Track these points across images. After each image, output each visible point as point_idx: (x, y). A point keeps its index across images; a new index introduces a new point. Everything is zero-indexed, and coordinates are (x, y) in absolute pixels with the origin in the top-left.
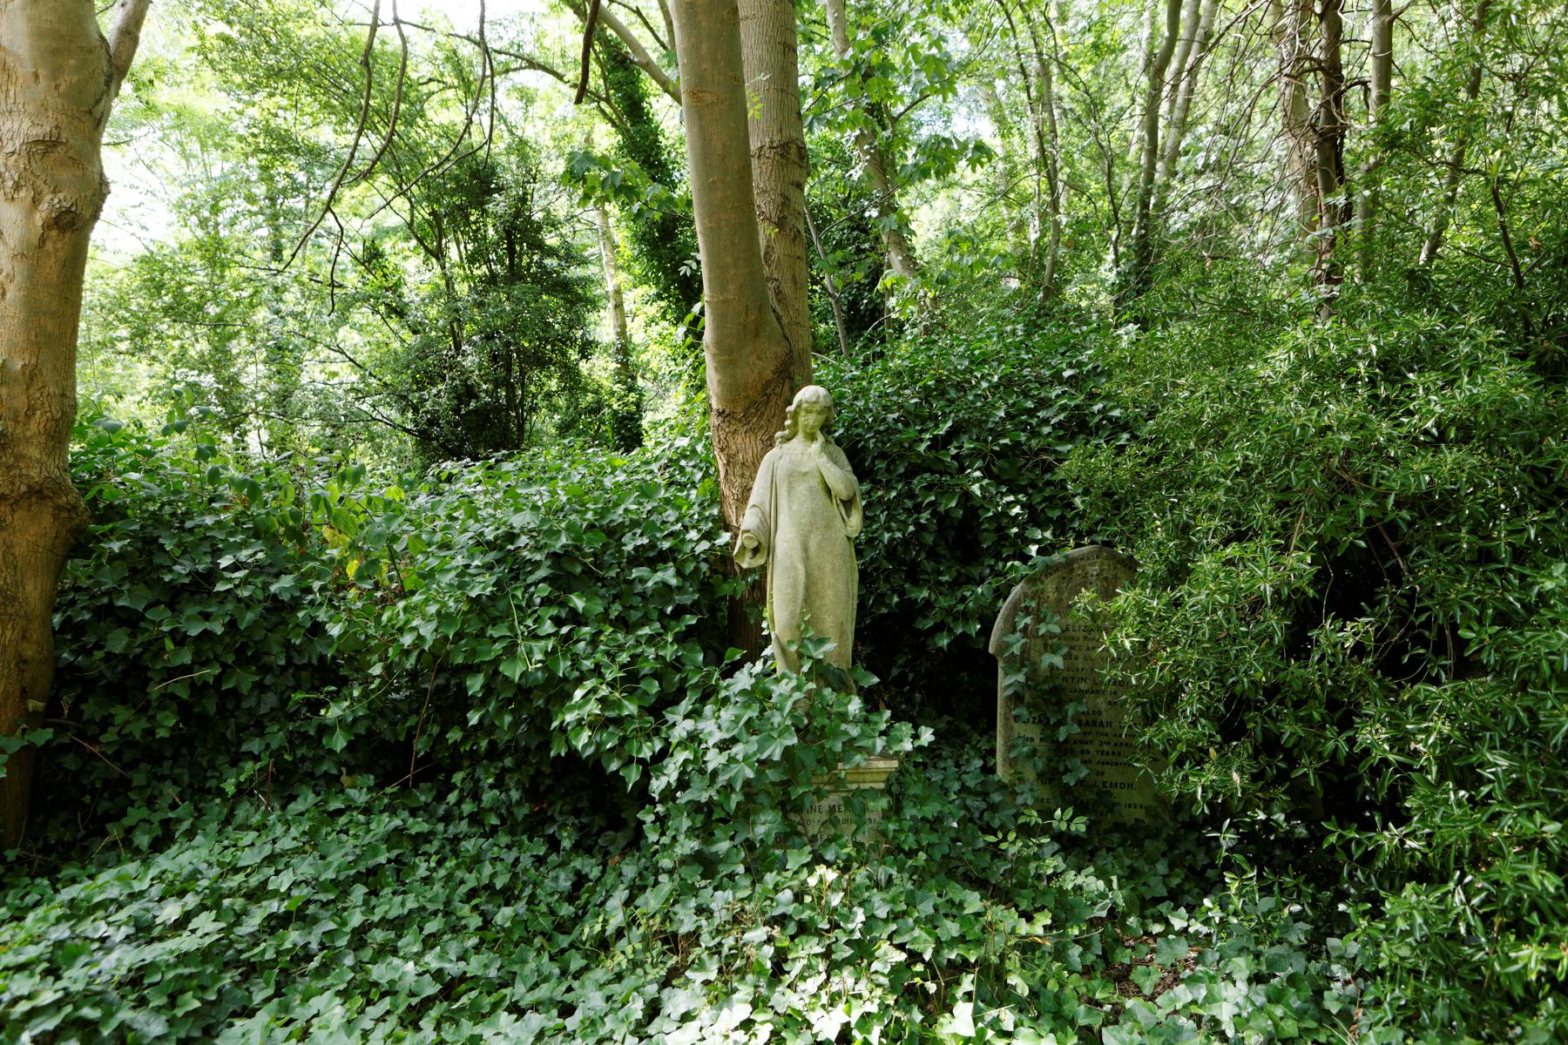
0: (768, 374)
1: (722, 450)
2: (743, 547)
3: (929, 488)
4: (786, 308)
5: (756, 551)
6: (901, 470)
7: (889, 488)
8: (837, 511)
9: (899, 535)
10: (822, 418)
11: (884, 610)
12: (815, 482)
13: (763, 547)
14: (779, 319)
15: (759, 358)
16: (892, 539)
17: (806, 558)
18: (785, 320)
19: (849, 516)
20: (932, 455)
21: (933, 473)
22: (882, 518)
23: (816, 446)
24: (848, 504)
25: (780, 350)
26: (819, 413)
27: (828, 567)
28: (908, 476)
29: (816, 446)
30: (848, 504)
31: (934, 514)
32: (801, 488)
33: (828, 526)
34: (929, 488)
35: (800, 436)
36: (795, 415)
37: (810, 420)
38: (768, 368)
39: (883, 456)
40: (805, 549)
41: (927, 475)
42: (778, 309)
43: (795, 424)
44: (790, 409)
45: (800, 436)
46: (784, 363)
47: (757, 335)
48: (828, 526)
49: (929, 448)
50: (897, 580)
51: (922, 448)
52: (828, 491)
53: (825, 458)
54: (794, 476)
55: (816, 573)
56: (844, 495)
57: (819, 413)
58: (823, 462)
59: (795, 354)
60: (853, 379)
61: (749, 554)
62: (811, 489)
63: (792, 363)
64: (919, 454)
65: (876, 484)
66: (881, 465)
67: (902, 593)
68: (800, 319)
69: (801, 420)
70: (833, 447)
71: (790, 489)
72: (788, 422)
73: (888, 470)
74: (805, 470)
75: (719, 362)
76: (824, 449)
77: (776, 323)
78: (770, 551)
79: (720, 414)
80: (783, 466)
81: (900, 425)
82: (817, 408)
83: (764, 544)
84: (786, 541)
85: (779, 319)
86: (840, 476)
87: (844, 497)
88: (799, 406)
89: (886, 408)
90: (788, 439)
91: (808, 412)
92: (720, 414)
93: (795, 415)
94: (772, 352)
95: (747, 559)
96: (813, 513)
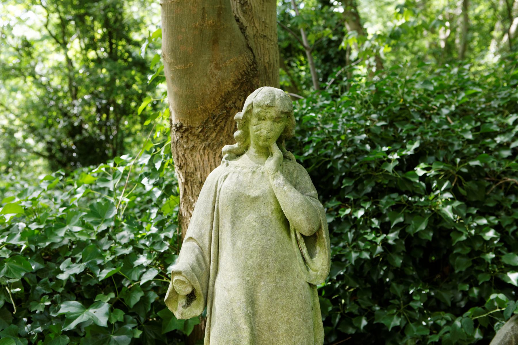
0: (228, 85)
1: (180, 168)
2: (174, 291)
3: (397, 208)
4: (251, 21)
5: (191, 297)
6: (369, 189)
7: (357, 206)
8: (295, 249)
9: (366, 255)
10: (278, 127)
11: (351, 331)
12: (268, 210)
13: (201, 293)
14: (243, 29)
15: (218, 67)
16: (359, 259)
17: (252, 316)
18: (250, 32)
19: (312, 255)
20: (399, 175)
21: (401, 193)
22: (350, 236)
23: (270, 164)
24: (311, 240)
25: (244, 59)
26: (275, 120)
27: (282, 328)
28: (374, 197)
29: (270, 164)
30: (311, 240)
31: (403, 234)
32: (250, 219)
33: (283, 270)
34: (397, 208)
35: (252, 150)
36: (246, 121)
37: (263, 129)
38: (229, 80)
39: (350, 175)
40: (252, 301)
41: (395, 195)
42: (243, 19)
43: (246, 135)
44: (239, 115)
45: (252, 150)
46: (246, 74)
47: (215, 42)
48: (283, 270)
49: (396, 168)
50: (365, 300)
51: (390, 168)
52: (286, 223)
53: (281, 180)
54: (240, 201)
55: (266, 335)
56: (306, 229)
57: (275, 120)
58: (279, 186)
59: (260, 68)
60: (323, 107)
61: (182, 301)
62: (262, 220)
63: (255, 76)
64: (386, 175)
65: (345, 203)
66: (347, 183)
67: (370, 315)
68: (267, 33)
69: (252, 129)
70: (294, 166)
71: (235, 219)
72: (237, 134)
73: (355, 189)
74: (254, 193)
75: (175, 72)
76: (280, 167)
77: (238, 32)
78: (208, 299)
79: (179, 129)
80: (227, 187)
81: (368, 147)
82: (272, 113)
83: (199, 291)
84: (228, 288)
85: (243, 29)
86: (299, 202)
87: (306, 233)
88: (249, 112)
89: (355, 132)
90: (238, 155)
91: (261, 119)
92: (179, 129)
93: (246, 121)
94: (233, 62)
95: (180, 308)
96: (264, 252)
